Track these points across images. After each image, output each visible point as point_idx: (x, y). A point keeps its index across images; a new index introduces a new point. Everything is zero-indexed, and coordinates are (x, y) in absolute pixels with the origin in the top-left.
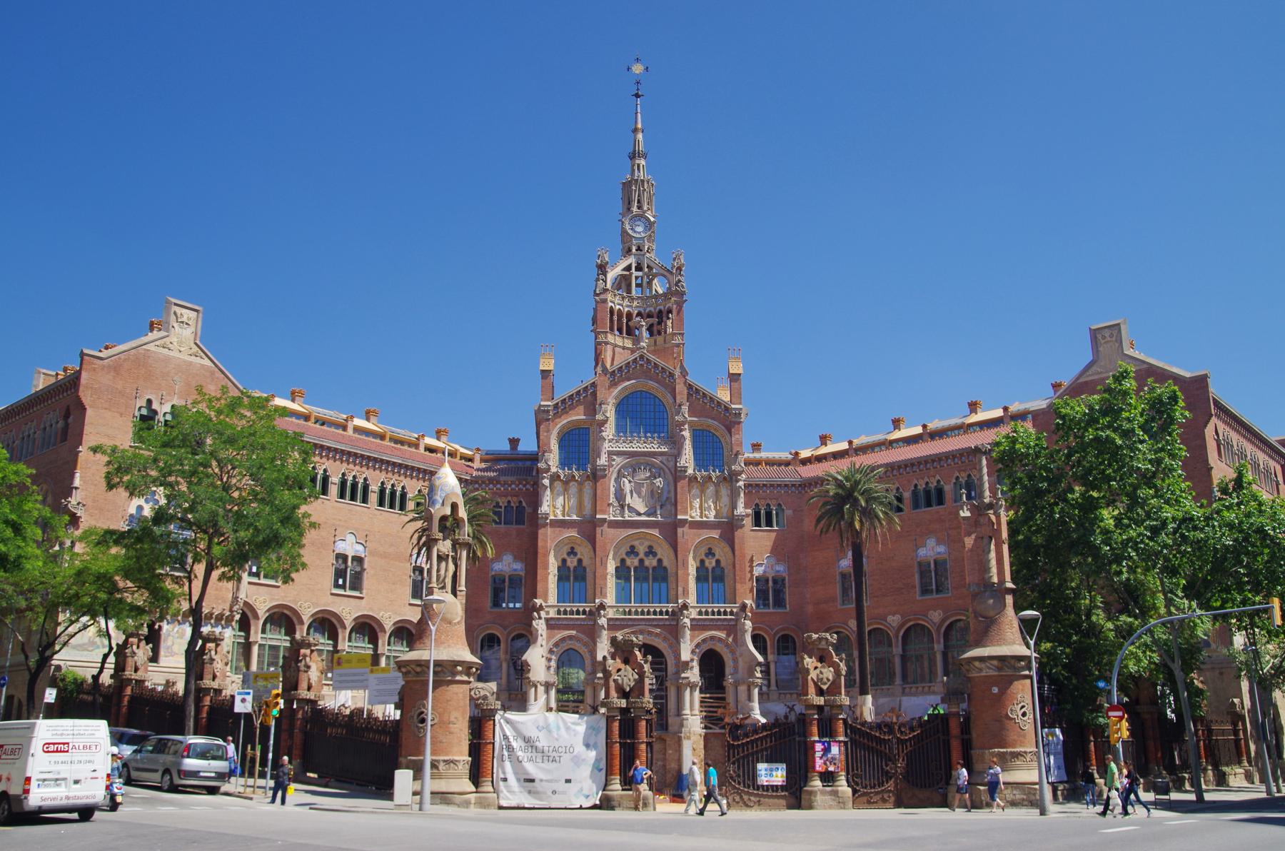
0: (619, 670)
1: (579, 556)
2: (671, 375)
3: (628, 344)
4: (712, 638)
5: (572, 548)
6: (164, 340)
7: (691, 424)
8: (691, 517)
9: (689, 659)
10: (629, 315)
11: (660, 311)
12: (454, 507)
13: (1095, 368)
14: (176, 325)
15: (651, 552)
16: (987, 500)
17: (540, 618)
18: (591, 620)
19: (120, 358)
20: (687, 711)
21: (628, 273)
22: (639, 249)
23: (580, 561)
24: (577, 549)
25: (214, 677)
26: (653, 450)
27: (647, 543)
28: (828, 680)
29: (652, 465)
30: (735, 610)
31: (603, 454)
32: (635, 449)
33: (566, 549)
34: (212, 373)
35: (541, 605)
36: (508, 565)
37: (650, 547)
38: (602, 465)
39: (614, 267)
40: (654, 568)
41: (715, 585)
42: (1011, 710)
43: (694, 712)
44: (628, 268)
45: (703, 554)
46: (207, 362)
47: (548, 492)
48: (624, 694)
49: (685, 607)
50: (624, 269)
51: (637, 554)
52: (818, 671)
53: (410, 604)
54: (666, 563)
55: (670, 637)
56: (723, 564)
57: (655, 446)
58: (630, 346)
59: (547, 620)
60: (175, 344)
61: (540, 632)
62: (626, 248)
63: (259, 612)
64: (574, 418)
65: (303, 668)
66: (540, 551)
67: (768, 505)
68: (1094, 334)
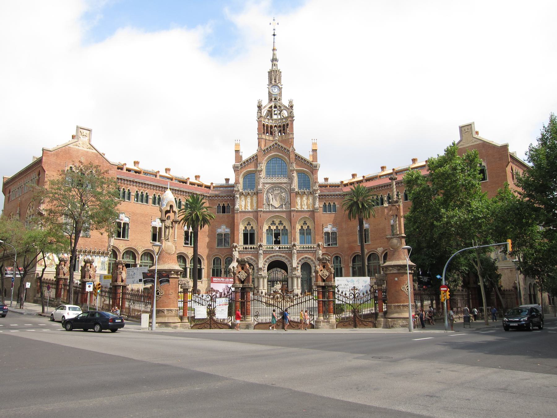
0: (239, 272)
1: (251, 225)
2: (288, 151)
3: (271, 138)
4: (306, 258)
5: (249, 222)
6: (77, 143)
7: (297, 171)
8: (297, 209)
9: (296, 267)
10: (271, 127)
11: (284, 125)
12: (171, 206)
13: (461, 143)
14: (81, 136)
15: (281, 223)
16: (395, 200)
17: (236, 251)
18: (256, 251)
19: (58, 151)
20: (295, 287)
22: (275, 99)
23: (252, 227)
24: (251, 223)
25: (90, 277)
26: (281, 182)
27: (279, 220)
28: (326, 275)
29: (281, 188)
30: (315, 246)
31: (260, 184)
33: (246, 223)
34: (97, 156)
35: (236, 246)
36: (223, 229)
37: (281, 221)
38: (260, 189)
39: (264, 107)
40: (282, 230)
41: (307, 236)
42: (403, 287)
43: (298, 288)
44: (271, 107)
45: (302, 224)
46: (94, 151)
47: (239, 200)
48: (242, 282)
49: (294, 245)
51: (275, 224)
52: (322, 272)
53: (183, 246)
54: (287, 228)
55: (289, 258)
56: (310, 228)
57: (282, 180)
58: (272, 139)
59: (239, 252)
60: (81, 144)
62: (270, 99)
63: (120, 250)
64: (249, 170)
65: (119, 273)
67: (329, 203)
68: (461, 128)
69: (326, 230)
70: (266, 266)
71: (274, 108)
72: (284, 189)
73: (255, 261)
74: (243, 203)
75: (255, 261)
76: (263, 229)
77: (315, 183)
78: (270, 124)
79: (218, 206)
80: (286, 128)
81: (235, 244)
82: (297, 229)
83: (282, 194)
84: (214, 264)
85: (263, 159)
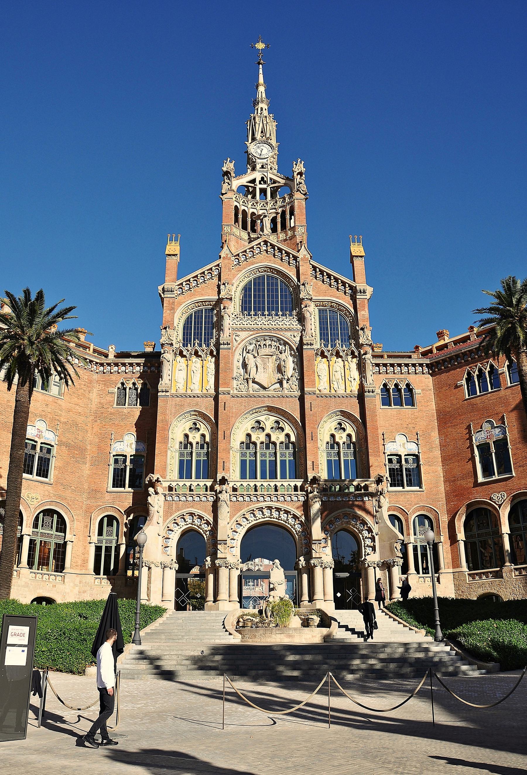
1: (201, 432)
2: (295, 258)
5: (195, 424)
8: (320, 391)
17: (157, 493)
21: (253, 185)
22: (262, 167)
32: (260, 326)
35: (158, 480)
37: (277, 422)
44: (253, 181)
50: (250, 182)
51: (263, 429)
57: (281, 324)
61: (156, 509)
66: (159, 424)
67: (396, 385)
69: (391, 448)
70: (239, 537)
71: (260, 183)
72: (285, 343)
73: (208, 523)
74: (180, 376)
75: (208, 523)
76: (232, 440)
77: (362, 329)
78: (252, 210)
79: (118, 388)
80: (288, 217)
81: (155, 477)
82: (319, 441)
83: (280, 356)
84: (100, 533)
85: (234, 276)
